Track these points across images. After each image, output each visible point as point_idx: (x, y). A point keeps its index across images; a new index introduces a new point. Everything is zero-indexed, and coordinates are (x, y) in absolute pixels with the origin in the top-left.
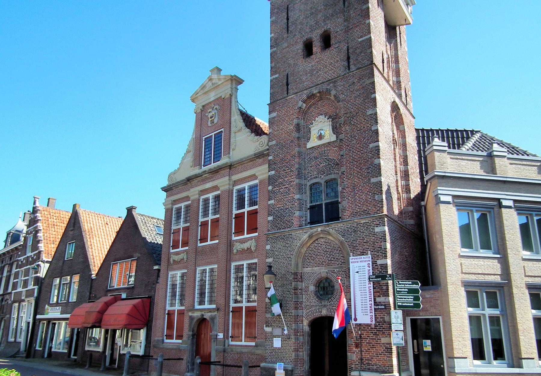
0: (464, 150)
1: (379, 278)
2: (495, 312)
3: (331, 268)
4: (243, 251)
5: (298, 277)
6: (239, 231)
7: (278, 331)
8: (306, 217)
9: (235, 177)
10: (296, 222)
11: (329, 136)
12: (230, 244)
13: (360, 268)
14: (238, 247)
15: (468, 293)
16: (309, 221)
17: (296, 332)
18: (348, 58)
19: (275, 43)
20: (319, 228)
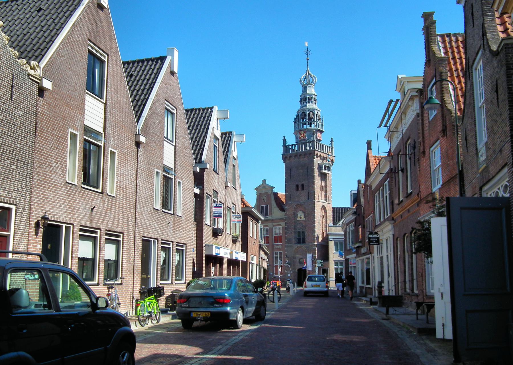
0: (338, 225)
1: (314, 259)
2: (341, 267)
4: (278, 248)
5: (294, 258)
6: (276, 242)
7: (289, 272)
9: (274, 224)
10: (294, 242)
11: (303, 218)
12: (273, 246)
13: (310, 256)
14: (276, 247)
15: (335, 263)
17: (294, 272)
19: (286, 181)
20: (300, 245)
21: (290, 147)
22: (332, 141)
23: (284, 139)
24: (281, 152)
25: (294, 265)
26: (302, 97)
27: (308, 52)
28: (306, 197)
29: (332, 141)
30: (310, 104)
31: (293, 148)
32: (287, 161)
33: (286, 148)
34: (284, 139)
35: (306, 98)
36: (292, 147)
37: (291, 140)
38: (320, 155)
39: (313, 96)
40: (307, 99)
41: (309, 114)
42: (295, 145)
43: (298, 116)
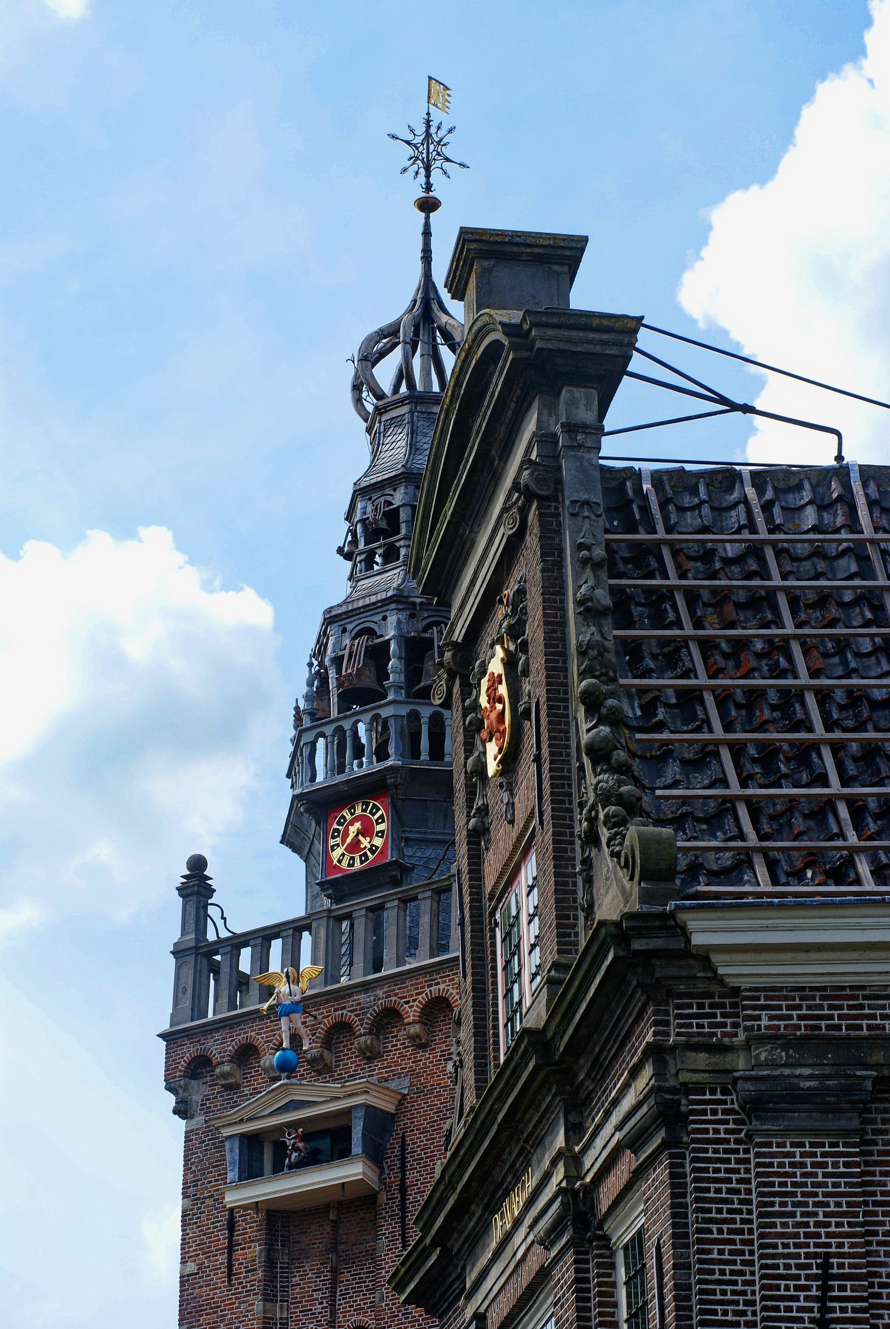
33: (201, 956)
36: (262, 961)
42: (291, 931)
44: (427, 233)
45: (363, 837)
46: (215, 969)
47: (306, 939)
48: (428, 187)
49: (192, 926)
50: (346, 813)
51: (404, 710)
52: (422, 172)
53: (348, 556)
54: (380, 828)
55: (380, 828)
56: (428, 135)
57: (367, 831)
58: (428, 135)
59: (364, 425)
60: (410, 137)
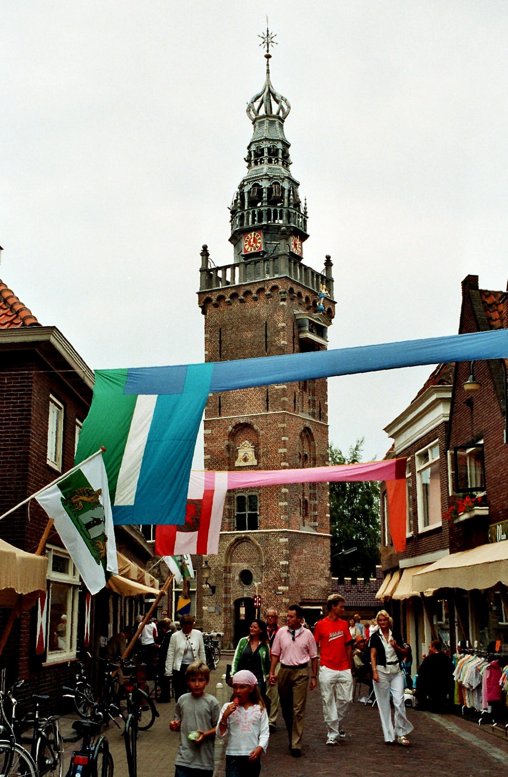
3: (251, 564)
8: (234, 523)
16: (236, 526)
18: (267, 400)
21: (220, 274)
22: (328, 263)
23: (205, 253)
24: (195, 282)
25: (227, 591)
26: (253, 148)
27: (268, 39)
28: (261, 403)
29: (328, 263)
30: (272, 166)
31: (228, 279)
32: (211, 309)
33: (208, 274)
34: (205, 253)
35: (262, 150)
36: (225, 275)
37: (224, 255)
38: (299, 295)
39: (280, 146)
40: (266, 150)
41: (270, 190)
42: (233, 267)
43: (242, 194)
44: (268, 65)
45: (254, 243)
46: (211, 276)
47: (237, 269)
48: (268, 51)
49: (205, 264)
50: (249, 235)
51: (266, 208)
52: (266, 47)
53: (247, 161)
54: (259, 241)
55: (259, 241)
56: (268, 35)
57: (255, 241)
58: (268, 35)
59: (252, 122)
60: (263, 36)
